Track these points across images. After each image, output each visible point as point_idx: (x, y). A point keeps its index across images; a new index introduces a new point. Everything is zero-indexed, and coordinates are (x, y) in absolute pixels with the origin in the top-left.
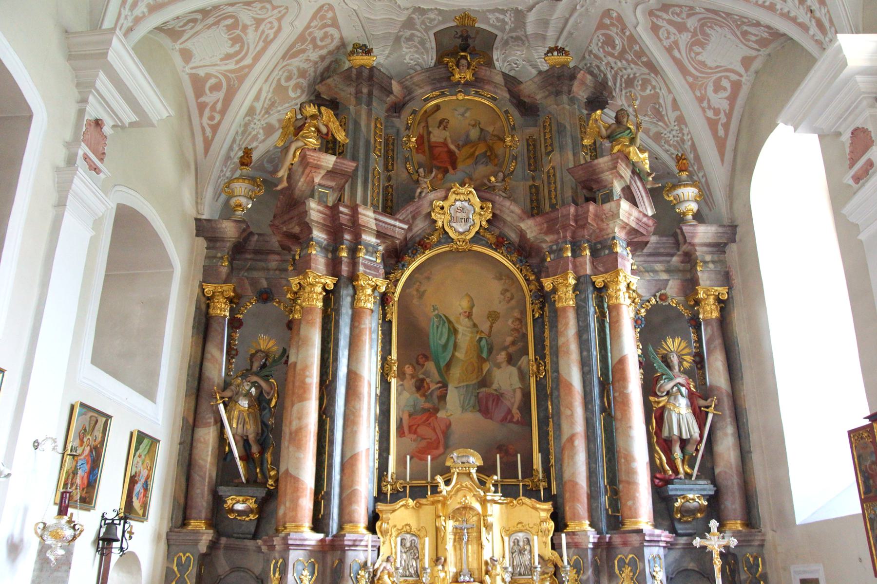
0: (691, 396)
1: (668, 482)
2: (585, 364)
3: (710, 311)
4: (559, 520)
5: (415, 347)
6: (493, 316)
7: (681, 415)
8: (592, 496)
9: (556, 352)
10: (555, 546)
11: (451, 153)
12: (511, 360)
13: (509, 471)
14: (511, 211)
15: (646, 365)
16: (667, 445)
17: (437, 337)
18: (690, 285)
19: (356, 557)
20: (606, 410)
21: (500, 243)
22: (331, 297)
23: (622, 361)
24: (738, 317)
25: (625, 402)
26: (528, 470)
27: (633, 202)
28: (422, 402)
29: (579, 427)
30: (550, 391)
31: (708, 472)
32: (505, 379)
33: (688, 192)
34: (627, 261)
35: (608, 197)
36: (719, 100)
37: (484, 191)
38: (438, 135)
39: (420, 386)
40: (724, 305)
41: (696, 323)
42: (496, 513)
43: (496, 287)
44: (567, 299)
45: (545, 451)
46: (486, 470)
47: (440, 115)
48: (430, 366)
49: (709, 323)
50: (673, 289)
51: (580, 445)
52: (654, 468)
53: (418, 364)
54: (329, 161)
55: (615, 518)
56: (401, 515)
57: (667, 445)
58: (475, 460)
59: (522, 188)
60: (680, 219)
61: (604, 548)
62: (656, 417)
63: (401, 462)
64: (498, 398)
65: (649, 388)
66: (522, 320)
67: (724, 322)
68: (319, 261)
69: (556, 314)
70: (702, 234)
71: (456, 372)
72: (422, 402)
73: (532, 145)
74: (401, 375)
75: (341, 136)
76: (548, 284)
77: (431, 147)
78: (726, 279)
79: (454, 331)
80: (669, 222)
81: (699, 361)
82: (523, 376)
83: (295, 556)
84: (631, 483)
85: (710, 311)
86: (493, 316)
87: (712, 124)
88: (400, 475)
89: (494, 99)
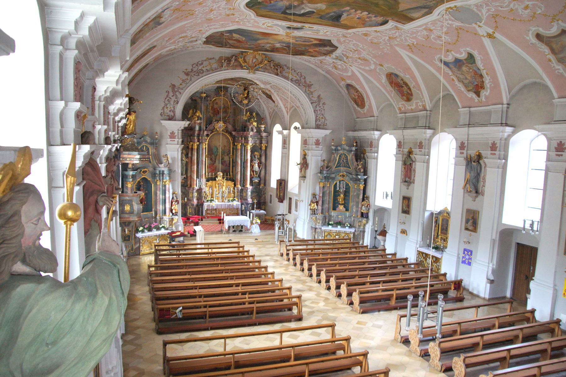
0: (258, 163)
1: (253, 178)
2: (241, 159)
3: (264, 148)
4: (235, 185)
5: (211, 152)
6: (225, 146)
7: (256, 167)
8: (240, 181)
9: (236, 156)
10: (234, 189)
11: (218, 111)
12: (228, 155)
13: (227, 175)
14: (230, 127)
15: (251, 157)
16: (253, 172)
17: (215, 150)
18: (261, 143)
19: (204, 191)
20: (244, 167)
21: (227, 131)
22: (198, 146)
23: (247, 160)
24: (268, 150)
25: (247, 166)
26: (230, 175)
27: (252, 130)
28: (212, 162)
29: (239, 170)
30: (235, 163)
31: (259, 176)
32: (226, 158)
33: (263, 126)
34: (250, 139)
35: (248, 130)
36: (271, 111)
37: (225, 122)
38: (216, 106)
39: (211, 159)
40: (266, 147)
41: (261, 149)
42: (225, 183)
43: (226, 140)
44: (239, 147)
45: (232, 172)
46: (223, 175)
47: (216, 101)
48: (213, 156)
49: (262, 152)
50: (258, 142)
51: (239, 173)
52: (251, 175)
53: (211, 155)
54: (199, 121)
55: (243, 184)
56: (209, 183)
57: (253, 172)
58: (222, 174)
59: (231, 120)
60: (261, 130)
61: (242, 190)
62: (252, 166)
63: (208, 173)
64: (225, 162)
65: (251, 161)
66: (230, 147)
67: (266, 150)
68: (196, 140)
69: (237, 150)
70: (264, 134)
71: (218, 157)
72: (212, 162)
73: (235, 110)
74: (208, 157)
75: (201, 116)
76: (236, 144)
77: (214, 109)
78: (267, 143)
79: (217, 149)
80: (259, 131)
81: (261, 156)
82: (230, 158)
83: (195, 191)
84: (247, 180)
85: (264, 148)
86: (225, 146)
87: (269, 113)
88: (208, 175)
89: (227, 98)
